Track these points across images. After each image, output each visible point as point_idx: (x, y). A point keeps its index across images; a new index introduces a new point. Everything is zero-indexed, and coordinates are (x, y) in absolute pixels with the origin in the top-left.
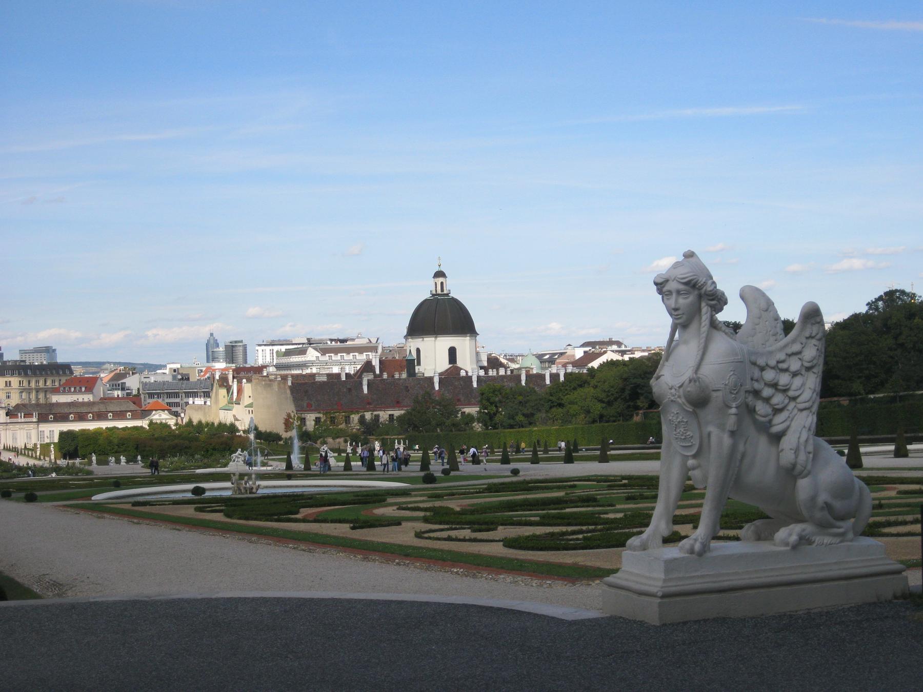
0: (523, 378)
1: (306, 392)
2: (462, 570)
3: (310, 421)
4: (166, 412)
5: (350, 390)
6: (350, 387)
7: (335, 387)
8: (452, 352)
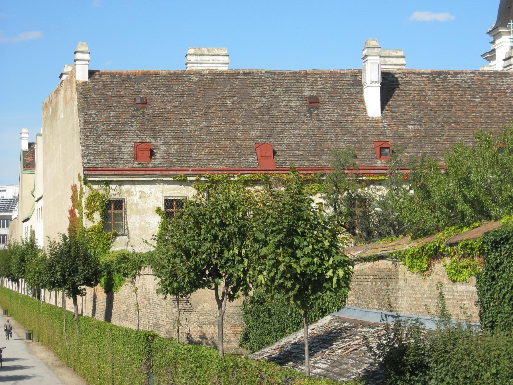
3: (141, 212)
6: (315, 94)
7: (258, 90)
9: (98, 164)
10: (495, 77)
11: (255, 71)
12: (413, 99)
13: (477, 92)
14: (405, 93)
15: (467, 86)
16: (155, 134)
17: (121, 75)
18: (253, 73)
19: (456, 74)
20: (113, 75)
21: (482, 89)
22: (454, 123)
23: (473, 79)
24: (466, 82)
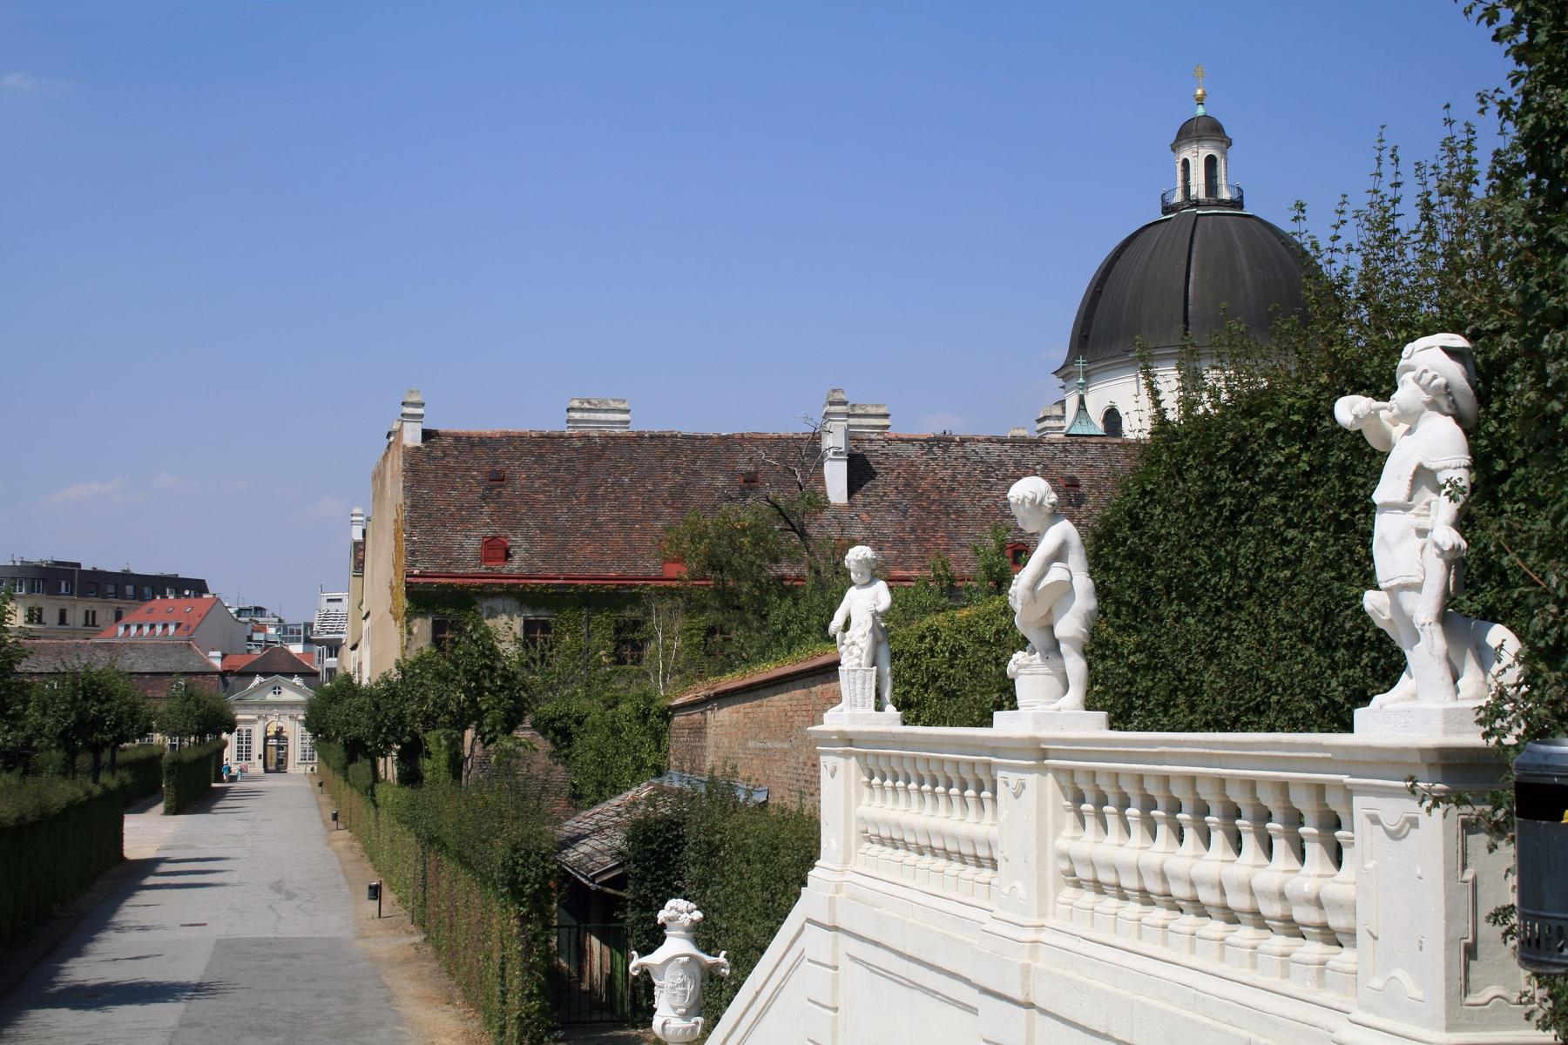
4: (297, 680)
6: (751, 468)
7: (669, 462)
9: (427, 568)
10: (1021, 447)
11: (667, 434)
12: (897, 478)
13: (992, 467)
14: (885, 468)
15: (978, 459)
16: (514, 523)
17: (469, 437)
18: (664, 436)
19: (963, 441)
20: (457, 438)
21: (1001, 464)
22: (955, 513)
23: (987, 449)
24: (977, 453)
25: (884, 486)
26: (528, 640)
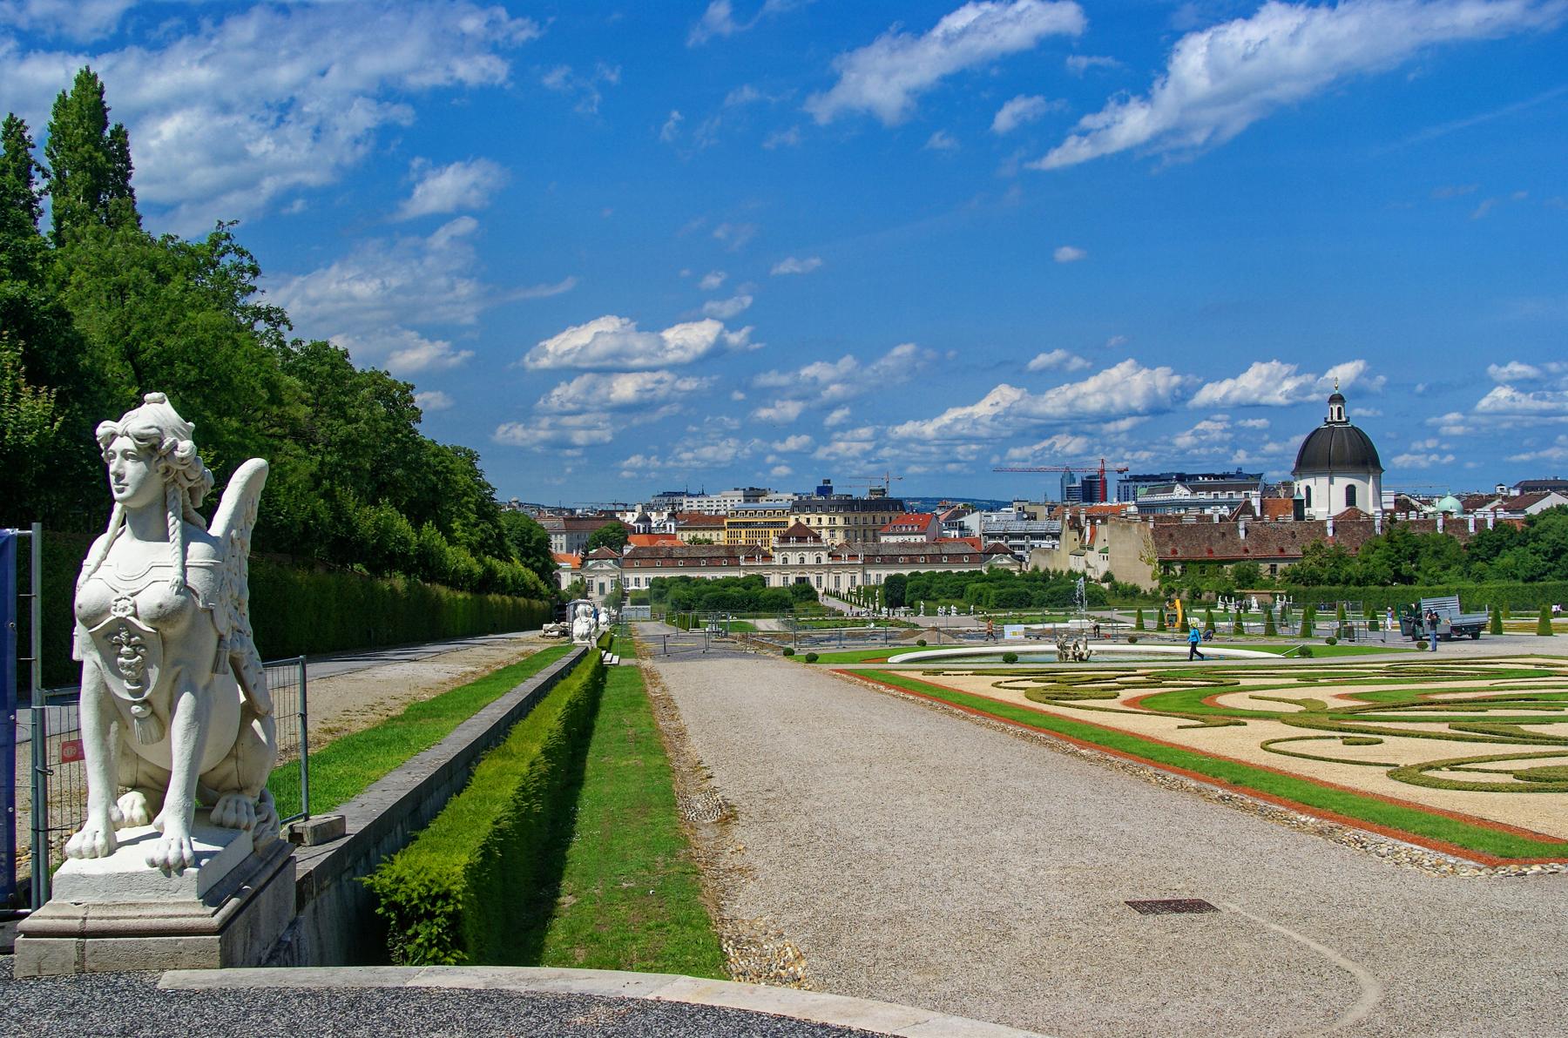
0: (1440, 523)
1: (1171, 535)
2: (1313, 820)
4: (1009, 556)
5: (1224, 534)
8: (1351, 491)
25: (1252, 533)
26: (1182, 571)
